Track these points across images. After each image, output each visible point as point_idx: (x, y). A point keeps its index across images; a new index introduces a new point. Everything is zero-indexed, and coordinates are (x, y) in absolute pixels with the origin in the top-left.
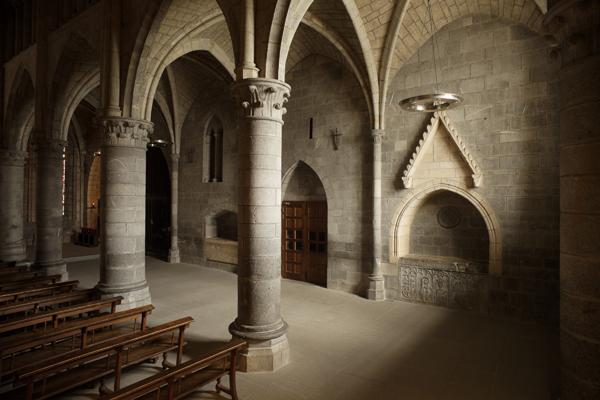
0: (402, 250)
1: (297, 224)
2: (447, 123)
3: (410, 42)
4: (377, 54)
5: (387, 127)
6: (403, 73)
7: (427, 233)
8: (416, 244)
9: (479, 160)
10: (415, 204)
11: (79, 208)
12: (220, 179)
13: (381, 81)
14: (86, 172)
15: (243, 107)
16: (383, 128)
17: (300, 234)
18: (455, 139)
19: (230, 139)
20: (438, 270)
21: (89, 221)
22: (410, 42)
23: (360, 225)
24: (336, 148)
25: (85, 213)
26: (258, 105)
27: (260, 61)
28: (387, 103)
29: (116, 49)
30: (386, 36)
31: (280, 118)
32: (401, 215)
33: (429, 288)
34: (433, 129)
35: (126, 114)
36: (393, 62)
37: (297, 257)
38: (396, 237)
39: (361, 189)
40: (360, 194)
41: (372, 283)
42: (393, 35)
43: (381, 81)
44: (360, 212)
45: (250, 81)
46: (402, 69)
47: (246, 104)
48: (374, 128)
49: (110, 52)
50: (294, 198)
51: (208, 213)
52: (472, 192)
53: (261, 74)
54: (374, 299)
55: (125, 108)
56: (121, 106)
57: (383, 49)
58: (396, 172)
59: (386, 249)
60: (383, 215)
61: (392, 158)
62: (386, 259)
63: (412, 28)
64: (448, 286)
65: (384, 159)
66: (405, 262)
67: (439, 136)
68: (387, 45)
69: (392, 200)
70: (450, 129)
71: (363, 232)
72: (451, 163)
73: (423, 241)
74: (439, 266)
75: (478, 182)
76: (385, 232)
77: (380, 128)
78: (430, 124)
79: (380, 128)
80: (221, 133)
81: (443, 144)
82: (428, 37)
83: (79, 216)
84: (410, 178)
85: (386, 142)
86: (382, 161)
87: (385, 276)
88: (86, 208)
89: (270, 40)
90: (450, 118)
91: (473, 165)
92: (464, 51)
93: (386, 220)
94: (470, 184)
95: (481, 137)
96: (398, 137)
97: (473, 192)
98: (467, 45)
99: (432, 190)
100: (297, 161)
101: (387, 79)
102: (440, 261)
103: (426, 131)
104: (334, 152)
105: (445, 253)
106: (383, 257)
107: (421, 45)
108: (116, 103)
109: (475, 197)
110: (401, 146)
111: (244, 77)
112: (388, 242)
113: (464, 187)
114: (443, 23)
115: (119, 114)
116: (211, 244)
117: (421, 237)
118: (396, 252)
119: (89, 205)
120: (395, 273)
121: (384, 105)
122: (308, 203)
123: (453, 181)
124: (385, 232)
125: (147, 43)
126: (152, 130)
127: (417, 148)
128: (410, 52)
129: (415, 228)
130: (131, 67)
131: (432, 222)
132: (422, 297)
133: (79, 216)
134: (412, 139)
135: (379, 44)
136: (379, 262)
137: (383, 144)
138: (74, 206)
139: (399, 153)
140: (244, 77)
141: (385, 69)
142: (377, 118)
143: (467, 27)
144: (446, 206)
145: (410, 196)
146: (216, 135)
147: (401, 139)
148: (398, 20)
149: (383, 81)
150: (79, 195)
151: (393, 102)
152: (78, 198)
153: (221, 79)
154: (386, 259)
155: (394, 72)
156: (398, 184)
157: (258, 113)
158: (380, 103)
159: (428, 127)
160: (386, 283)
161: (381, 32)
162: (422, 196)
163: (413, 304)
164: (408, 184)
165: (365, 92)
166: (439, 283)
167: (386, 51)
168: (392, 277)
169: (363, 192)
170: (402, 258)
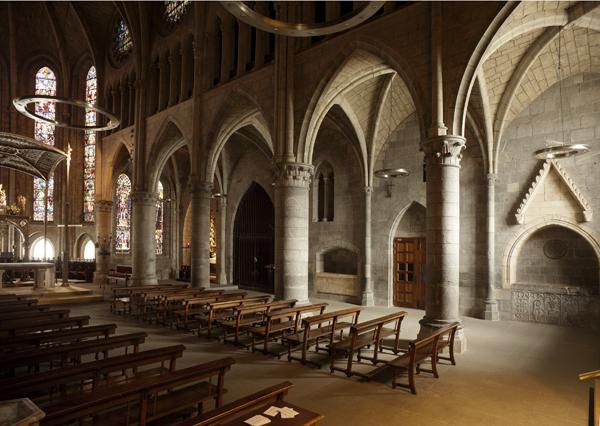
0: (513, 280)
1: (409, 258)
2: (558, 168)
3: (523, 97)
4: (494, 108)
6: (515, 124)
7: (533, 264)
8: (523, 273)
9: (590, 198)
10: (526, 236)
11: (175, 247)
12: (331, 218)
14: (182, 214)
15: (436, 156)
17: (411, 267)
18: (567, 181)
19: (341, 181)
20: (547, 293)
21: (184, 261)
22: (523, 97)
23: (474, 257)
24: (389, 196)
25: (181, 252)
26: (449, 155)
27: (448, 121)
29: (291, 107)
31: (458, 164)
32: (513, 247)
33: (542, 309)
34: (545, 173)
35: (299, 160)
36: (508, 116)
37: (409, 287)
38: (508, 267)
39: (474, 226)
40: (474, 230)
41: (487, 306)
42: (512, 92)
43: (496, 132)
44: (474, 246)
46: (514, 120)
47: (438, 154)
48: (488, 172)
49: (286, 108)
50: (405, 235)
51: (319, 249)
52: (582, 226)
53: (450, 131)
54: (490, 318)
55: (299, 155)
56: (296, 155)
57: (499, 104)
58: (509, 209)
59: (499, 277)
60: (496, 248)
61: (504, 198)
62: (499, 286)
63: (527, 87)
65: (497, 199)
66: (517, 288)
67: (550, 178)
68: (504, 101)
69: (506, 234)
70: (562, 173)
71: (476, 263)
72: (561, 202)
73: (529, 271)
74: (549, 290)
75: (589, 216)
76: (498, 262)
78: (543, 168)
79: (494, 173)
80: (331, 176)
81: (554, 185)
82: (540, 93)
83: (175, 255)
84: (523, 215)
85: (498, 184)
87: (498, 300)
88: (181, 248)
89: (457, 106)
90: (562, 166)
91: (584, 203)
92: (574, 105)
93: (499, 252)
94: (581, 219)
95: (591, 179)
97: (583, 226)
98: (577, 100)
99: (542, 226)
100: (412, 201)
101: (502, 130)
102: (551, 288)
103: (539, 174)
104: (388, 200)
105: (552, 280)
106: (496, 283)
107: (532, 99)
108: (291, 151)
109: (585, 231)
110: (514, 188)
111: (440, 134)
112: (500, 271)
113: (575, 222)
114: (555, 81)
115: (293, 160)
116: (322, 278)
117: (528, 268)
118: (508, 279)
119: (184, 245)
120: (508, 297)
122: (422, 240)
123: (563, 215)
124: (498, 262)
125: (319, 102)
126: (313, 173)
127: (530, 190)
128: (522, 106)
129: (522, 260)
130: (305, 121)
131: (539, 253)
132: (534, 318)
133: (175, 255)
134: (524, 181)
135: (496, 100)
136: (492, 287)
137: (496, 187)
138: (170, 245)
139: (512, 194)
140: (440, 134)
142: (491, 163)
143: (579, 84)
144: (556, 241)
145: (522, 231)
146: (325, 179)
148: (518, 81)
149: (498, 131)
150: (175, 235)
152: (174, 238)
153: (339, 128)
154: (499, 286)
156: (511, 220)
157: (448, 161)
158: (494, 150)
159: (541, 171)
160: (499, 308)
161: (500, 90)
162: (532, 231)
163: (525, 324)
164: (520, 222)
165: (480, 141)
166: (551, 305)
167: (502, 106)
168: (505, 301)
169: (476, 228)
170: (514, 285)
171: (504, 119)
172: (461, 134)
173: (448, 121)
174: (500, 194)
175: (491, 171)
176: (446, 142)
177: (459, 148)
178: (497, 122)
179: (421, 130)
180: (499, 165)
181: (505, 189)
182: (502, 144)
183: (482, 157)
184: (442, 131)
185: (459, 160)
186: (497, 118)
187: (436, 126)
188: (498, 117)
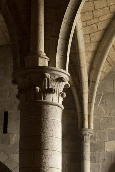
4: (90, 56)
5: (95, 123)
13: (92, 82)
15: (35, 90)
16: (92, 127)
26: (51, 91)
27: (51, 51)
28: (96, 104)
30: (100, 42)
36: (104, 68)
43: (92, 82)
45: (43, 69)
46: (111, 72)
47: (38, 88)
53: (52, 62)
61: (101, 158)
65: (93, 159)
68: (101, 50)
77: (89, 127)
85: (95, 142)
86: (91, 161)
89: (60, 36)
96: (107, 138)
101: (98, 81)
111: (40, 64)
121: (93, 105)
135: (92, 47)
139: (109, 153)
140: (40, 64)
141: (97, 71)
147: (110, 140)
149: (94, 82)
151: (102, 103)
155: (103, 76)
158: (90, 103)
161: (97, 37)
167: (99, 55)
171: (101, 69)
172: (65, 69)
173: (51, 51)
174: (96, 153)
175: (86, 126)
176: (48, 75)
177: (62, 85)
178: (93, 71)
179: (15, 59)
180: (96, 120)
181: (102, 148)
182: (98, 96)
183: (75, 109)
184: (44, 62)
185: (61, 100)
186: (94, 67)
187: (36, 55)
188: (95, 66)
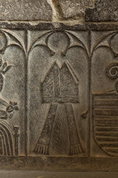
64: (23, 86)
